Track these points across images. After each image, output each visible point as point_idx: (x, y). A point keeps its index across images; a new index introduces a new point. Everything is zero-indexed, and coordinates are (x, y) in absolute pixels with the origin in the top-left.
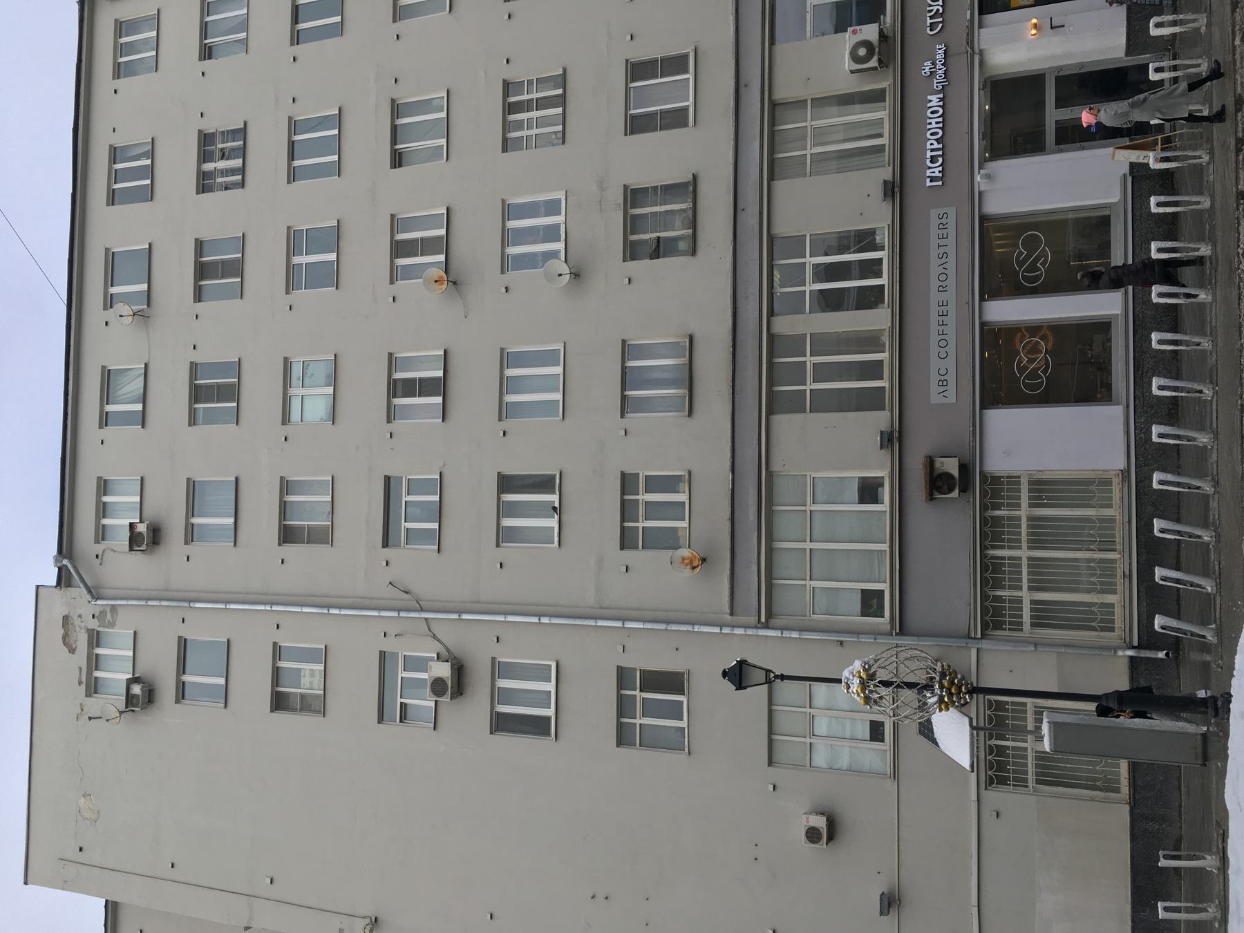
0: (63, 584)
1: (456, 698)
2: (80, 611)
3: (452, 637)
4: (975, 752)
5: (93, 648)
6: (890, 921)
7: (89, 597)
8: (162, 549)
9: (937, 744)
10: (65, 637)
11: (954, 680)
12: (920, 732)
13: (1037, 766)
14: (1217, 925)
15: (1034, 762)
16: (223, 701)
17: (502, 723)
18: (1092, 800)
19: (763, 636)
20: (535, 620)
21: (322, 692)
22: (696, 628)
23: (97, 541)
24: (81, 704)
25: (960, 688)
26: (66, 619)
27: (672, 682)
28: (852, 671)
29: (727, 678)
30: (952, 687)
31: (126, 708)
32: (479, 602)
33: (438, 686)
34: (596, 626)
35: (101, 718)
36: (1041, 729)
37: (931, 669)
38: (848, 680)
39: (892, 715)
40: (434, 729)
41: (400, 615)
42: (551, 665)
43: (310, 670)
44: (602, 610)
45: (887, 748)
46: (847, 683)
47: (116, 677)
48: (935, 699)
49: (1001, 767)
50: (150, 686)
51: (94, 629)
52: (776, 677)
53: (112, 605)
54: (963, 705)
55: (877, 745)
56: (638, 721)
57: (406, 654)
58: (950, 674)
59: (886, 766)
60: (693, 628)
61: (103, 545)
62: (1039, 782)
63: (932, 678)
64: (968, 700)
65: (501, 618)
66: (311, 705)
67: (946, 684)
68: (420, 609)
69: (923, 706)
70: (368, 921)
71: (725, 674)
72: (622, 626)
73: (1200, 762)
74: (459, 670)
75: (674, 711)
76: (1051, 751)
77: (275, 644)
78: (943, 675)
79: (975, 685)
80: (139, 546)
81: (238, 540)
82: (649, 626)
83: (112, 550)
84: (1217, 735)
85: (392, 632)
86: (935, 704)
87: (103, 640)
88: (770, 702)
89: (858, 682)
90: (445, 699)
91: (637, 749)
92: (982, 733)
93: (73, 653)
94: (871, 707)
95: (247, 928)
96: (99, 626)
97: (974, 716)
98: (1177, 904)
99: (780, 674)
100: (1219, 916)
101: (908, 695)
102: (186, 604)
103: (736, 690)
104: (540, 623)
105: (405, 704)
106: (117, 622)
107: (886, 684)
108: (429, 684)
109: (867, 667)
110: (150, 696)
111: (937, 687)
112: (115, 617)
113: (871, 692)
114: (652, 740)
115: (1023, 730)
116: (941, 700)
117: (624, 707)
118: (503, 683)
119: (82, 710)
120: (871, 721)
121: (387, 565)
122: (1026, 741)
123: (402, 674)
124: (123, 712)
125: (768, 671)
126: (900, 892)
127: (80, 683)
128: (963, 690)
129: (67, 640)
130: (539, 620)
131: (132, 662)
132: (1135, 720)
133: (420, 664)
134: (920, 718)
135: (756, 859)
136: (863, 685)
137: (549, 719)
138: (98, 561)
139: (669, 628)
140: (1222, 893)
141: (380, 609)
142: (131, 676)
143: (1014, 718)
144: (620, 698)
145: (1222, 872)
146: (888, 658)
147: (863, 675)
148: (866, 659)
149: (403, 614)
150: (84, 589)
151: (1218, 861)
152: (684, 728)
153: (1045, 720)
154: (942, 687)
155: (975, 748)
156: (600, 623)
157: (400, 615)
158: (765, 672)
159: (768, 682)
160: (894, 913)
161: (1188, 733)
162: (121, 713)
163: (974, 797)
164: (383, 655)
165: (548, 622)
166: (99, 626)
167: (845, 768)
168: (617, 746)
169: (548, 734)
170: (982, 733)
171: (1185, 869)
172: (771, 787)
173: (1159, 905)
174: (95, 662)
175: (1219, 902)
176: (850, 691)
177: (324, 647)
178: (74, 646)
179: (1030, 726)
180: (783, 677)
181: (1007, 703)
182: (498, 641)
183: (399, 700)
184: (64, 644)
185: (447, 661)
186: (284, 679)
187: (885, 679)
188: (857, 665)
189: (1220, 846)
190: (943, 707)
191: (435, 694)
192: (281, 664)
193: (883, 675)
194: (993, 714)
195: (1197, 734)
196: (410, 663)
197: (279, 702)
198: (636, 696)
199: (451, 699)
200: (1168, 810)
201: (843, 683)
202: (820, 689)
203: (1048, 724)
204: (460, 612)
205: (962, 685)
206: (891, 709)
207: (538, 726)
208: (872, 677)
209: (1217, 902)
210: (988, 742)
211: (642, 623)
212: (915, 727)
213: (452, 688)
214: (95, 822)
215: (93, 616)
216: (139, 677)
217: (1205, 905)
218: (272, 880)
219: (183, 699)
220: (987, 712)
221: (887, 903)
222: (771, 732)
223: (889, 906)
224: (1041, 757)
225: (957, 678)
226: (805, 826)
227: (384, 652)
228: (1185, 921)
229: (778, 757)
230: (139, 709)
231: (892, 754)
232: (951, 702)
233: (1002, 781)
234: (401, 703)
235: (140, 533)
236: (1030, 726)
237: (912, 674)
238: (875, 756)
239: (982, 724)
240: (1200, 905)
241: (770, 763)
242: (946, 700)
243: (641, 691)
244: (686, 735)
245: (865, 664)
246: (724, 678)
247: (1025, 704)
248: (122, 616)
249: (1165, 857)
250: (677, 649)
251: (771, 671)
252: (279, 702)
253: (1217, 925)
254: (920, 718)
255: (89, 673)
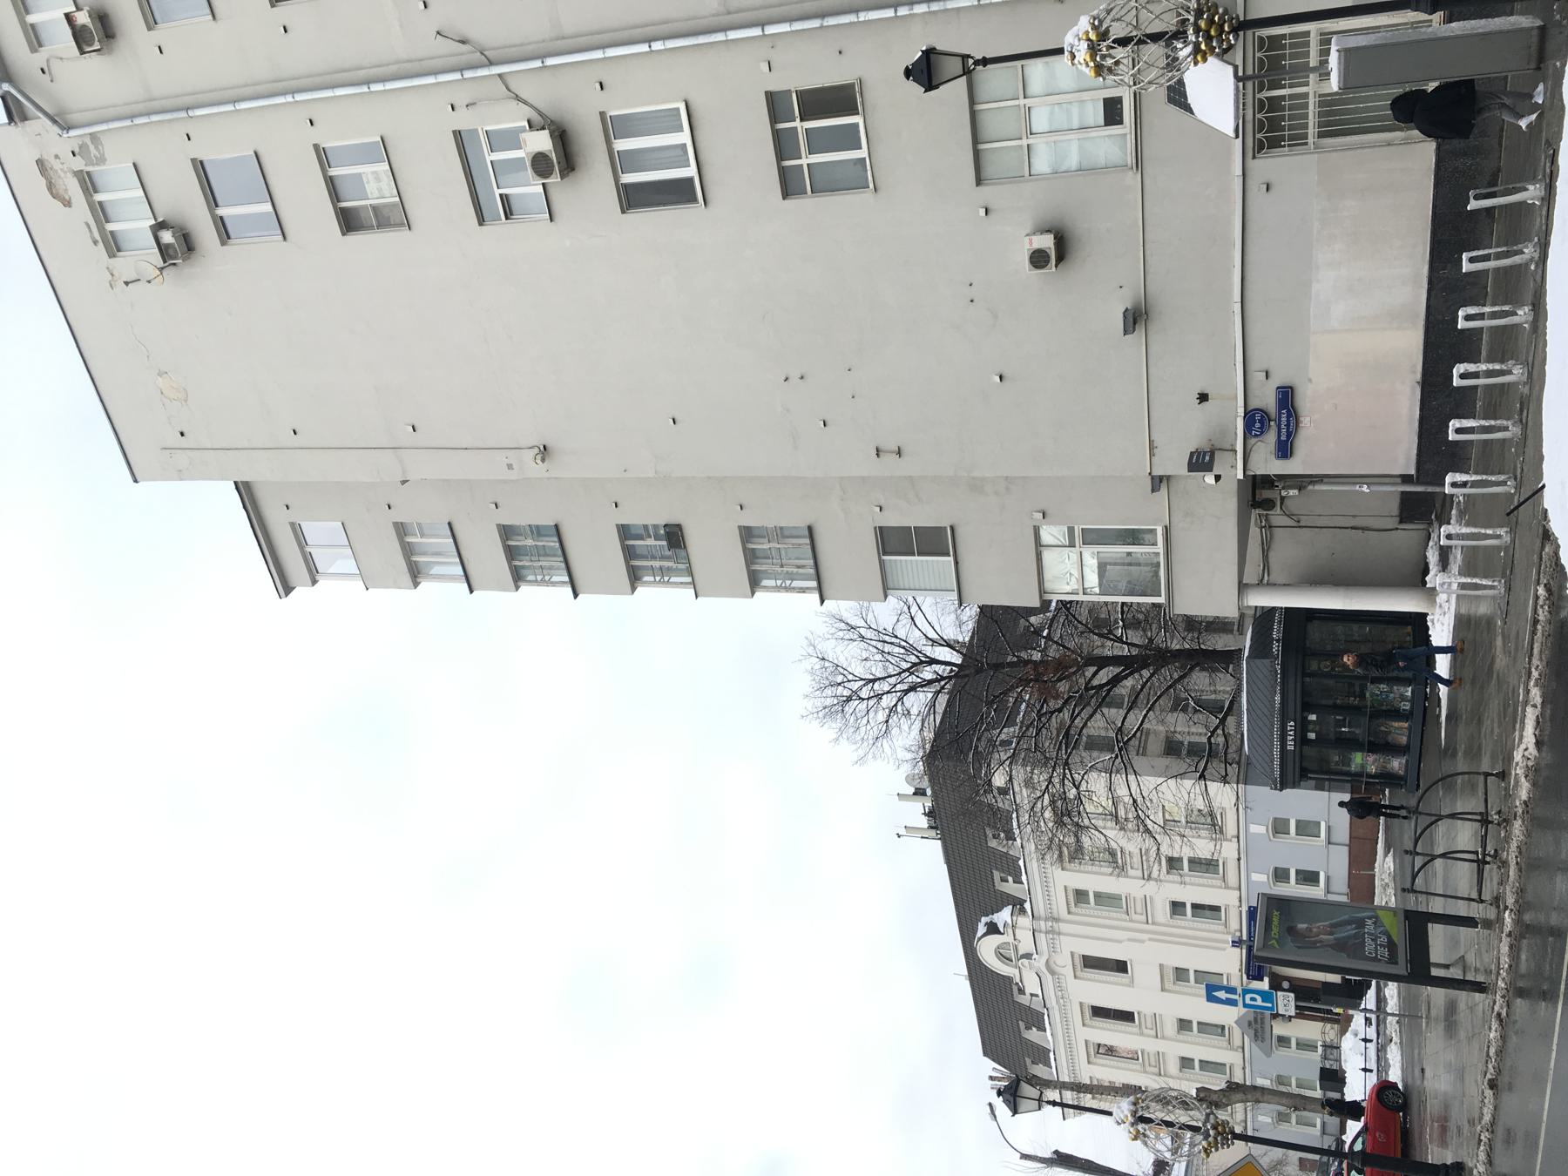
0: (16, 119)
1: (568, 175)
2: (55, 151)
3: (542, 92)
4: (1241, 111)
5: (91, 196)
6: (1138, 337)
7: (56, 129)
8: (121, 43)
9: (1193, 114)
10: (51, 187)
11: (1214, 17)
12: (1171, 100)
13: (1320, 114)
14: (1533, 267)
15: (1317, 110)
16: (279, 232)
17: (633, 198)
18: (1389, 145)
19: (953, 9)
20: (644, 48)
21: (397, 199)
22: (863, 16)
23: (33, 50)
24: (108, 268)
25: (1222, 26)
26: (40, 163)
27: (840, 100)
28: (1077, 34)
29: (911, 78)
30: (1211, 28)
31: (165, 262)
32: (563, 38)
33: (540, 164)
34: (727, 41)
35: (139, 280)
36: (1328, 63)
37: (1182, 8)
38: (1072, 48)
39: (1132, 83)
40: (551, 221)
41: (465, 77)
42: (678, 109)
43: (373, 173)
44: (731, 16)
45: (1127, 130)
46: (1071, 52)
47: (135, 225)
48: (1189, 49)
49: (1274, 125)
50: (182, 229)
51: (82, 171)
52: (977, 63)
53: (90, 134)
54: (1226, 51)
55: (1115, 130)
56: (804, 162)
57: (488, 128)
58: (1209, 10)
59: (1126, 155)
60: (858, 17)
61: (43, 54)
62: (1321, 135)
63: (1184, 21)
64: (1233, 42)
65: (598, 54)
66: (389, 217)
67: (1202, 24)
68: (487, 63)
69: (1173, 63)
70: (536, 450)
71: (908, 73)
72: (761, 34)
73: (1533, 65)
74: (562, 137)
75: (849, 138)
76: (1340, 89)
77: (316, 147)
78: (1199, 13)
79: (1242, 19)
80: (91, 45)
81: (217, 11)
82: (798, 26)
83: (58, 58)
84: (1561, 22)
85: (460, 102)
86: (1188, 57)
87: (99, 181)
88: (972, 101)
89: (1086, 46)
90: (554, 179)
91: (810, 197)
92: (1250, 84)
93: (70, 207)
94: (1104, 79)
95: (404, 482)
96: (86, 165)
97: (1239, 62)
98: (1486, 252)
99: (981, 58)
100: (1536, 256)
101: (1154, 51)
102: (183, 114)
103: (925, 91)
104: (652, 51)
105: (506, 195)
106: (106, 156)
107: (1123, 42)
108: (528, 163)
109: (1096, 23)
110: (188, 243)
111: (1191, 31)
112: (100, 147)
113: (1104, 57)
114: (828, 183)
115: (1306, 69)
116: (1197, 46)
117: (783, 146)
118: (621, 145)
119: (112, 275)
120: (1104, 99)
121: (426, 7)
122: (1307, 84)
123: (491, 157)
124: (162, 268)
125: (965, 57)
126: (1148, 305)
127: (95, 242)
128: (1226, 29)
129: (54, 192)
130: (650, 47)
131: (141, 189)
132: (1453, 24)
133: (508, 139)
134: (1168, 81)
135: (972, 301)
136: (1093, 49)
137: (690, 180)
138: (46, 77)
139: (825, 24)
140: (1544, 227)
141: (435, 73)
142: (153, 222)
143: (1292, 56)
144: (778, 136)
145: (1546, 203)
146: (1125, 4)
147: (1093, 36)
148: (1095, 12)
149: (468, 74)
150: (48, 122)
151: (1543, 190)
152: (864, 159)
153: (1334, 48)
154: (1197, 30)
155: (1241, 96)
156: (733, 35)
157: (465, 77)
158: (960, 58)
159: (967, 72)
160: (1140, 333)
161: (1522, 30)
162: (161, 269)
163: (1239, 171)
164: (458, 135)
165: (663, 48)
166: (86, 165)
167: (1074, 168)
168: (784, 199)
169: (695, 200)
170: (1250, 84)
171: (1501, 207)
172: (982, 212)
173: (1463, 256)
174: (101, 213)
175: (1539, 240)
176: (1076, 61)
177: (380, 140)
178: (67, 198)
179: (1313, 62)
180: (985, 62)
181: (1283, 36)
182: (602, 88)
183: (497, 192)
184: (52, 193)
185: (543, 128)
186: (344, 189)
187: (1121, 35)
188: (1084, 24)
189: (1548, 171)
190: (1199, 58)
191: (539, 175)
192: (333, 172)
193: (1118, 31)
194: (1265, 117)
195: (1532, 28)
196: (498, 140)
197: (349, 221)
198: (796, 128)
199: (562, 178)
200: (1486, 139)
201: (1066, 52)
202: (1036, 68)
203: (1337, 54)
204: (542, 57)
205: (1225, 22)
206: (1131, 75)
207: (679, 193)
208: (1103, 36)
209: (1536, 240)
210: (1258, 96)
211: (788, 24)
212: (1163, 93)
213: (559, 163)
214: (186, 401)
215: (74, 155)
216: (163, 221)
217: (1520, 246)
218: (413, 427)
219: (229, 238)
220: (1258, 55)
221: (1132, 320)
222: (976, 140)
223: (1135, 323)
224: (1326, 102)
225: (1217, 13)
226: (1028, 250)
227: (459, 132)
228: (1494, 269)
229: (989, 170)
230: (181, 261)
231: (1133, 137)
232: (1209, 50)
233: (1274, 143)
234: (501, 195)
235: (84, 26)
236: (1313, 62)
237: (1157, 20)
238: (1111, 145)
239: (1250, 72)
240: (1515, 248)
241: (979, 181)
242: (1203, 47)
243: (802, 120)
244: (868, 167)
245: (1094, 19)
246: (908, 79)
247: (1307, 34)
248: (110, 146)
249: (1476, 198)
250: (840, 52)
251: (969, 56)
252: (349, 221)
253: (1533, 267)
254: (1168, 81)
255: (101, 230)
